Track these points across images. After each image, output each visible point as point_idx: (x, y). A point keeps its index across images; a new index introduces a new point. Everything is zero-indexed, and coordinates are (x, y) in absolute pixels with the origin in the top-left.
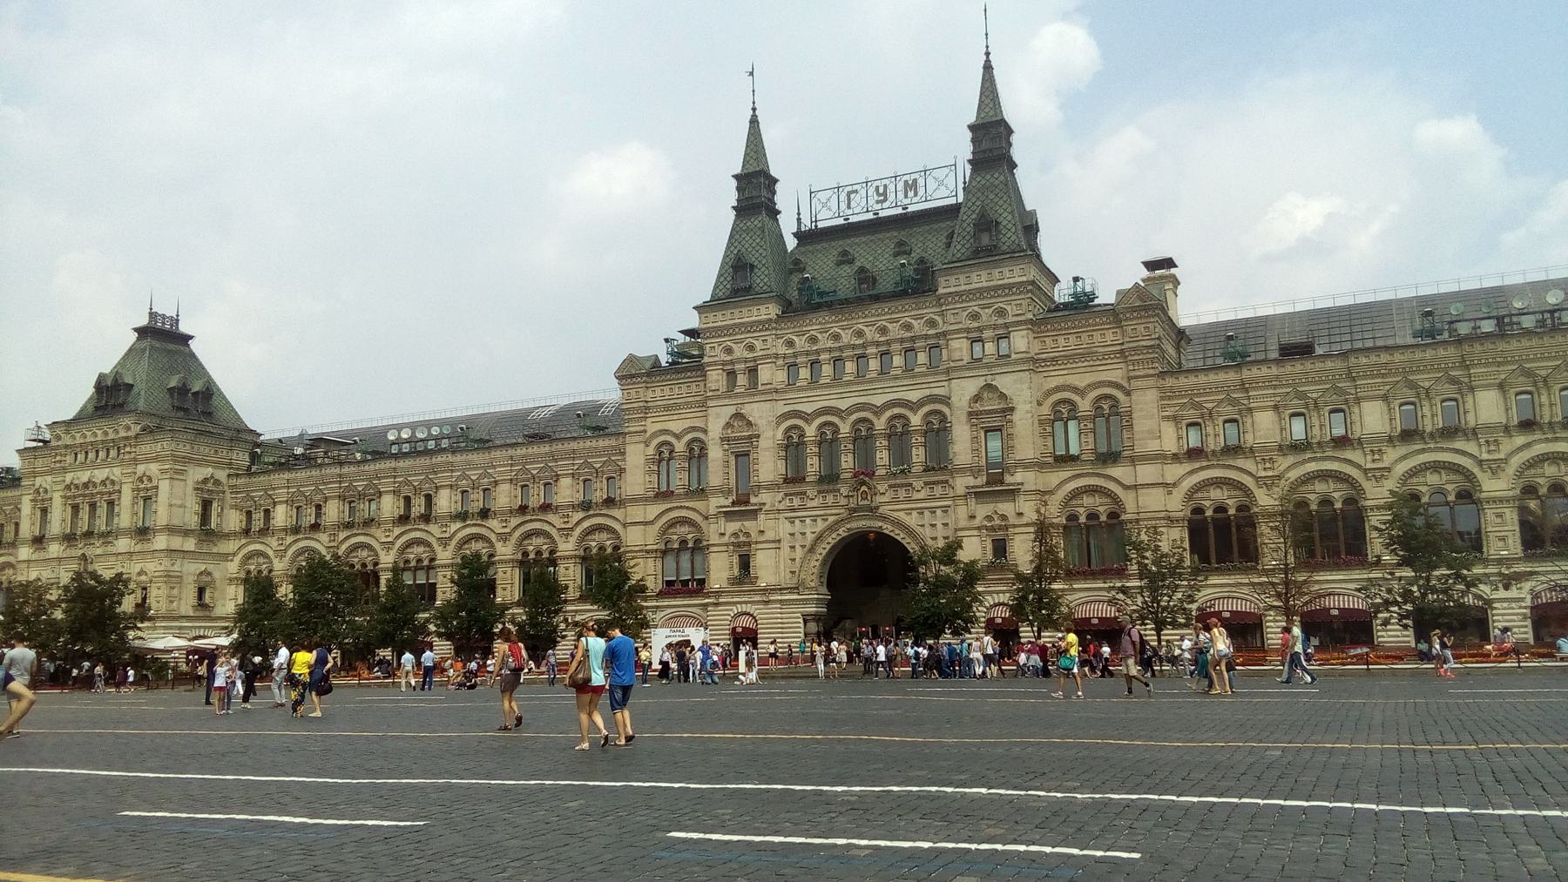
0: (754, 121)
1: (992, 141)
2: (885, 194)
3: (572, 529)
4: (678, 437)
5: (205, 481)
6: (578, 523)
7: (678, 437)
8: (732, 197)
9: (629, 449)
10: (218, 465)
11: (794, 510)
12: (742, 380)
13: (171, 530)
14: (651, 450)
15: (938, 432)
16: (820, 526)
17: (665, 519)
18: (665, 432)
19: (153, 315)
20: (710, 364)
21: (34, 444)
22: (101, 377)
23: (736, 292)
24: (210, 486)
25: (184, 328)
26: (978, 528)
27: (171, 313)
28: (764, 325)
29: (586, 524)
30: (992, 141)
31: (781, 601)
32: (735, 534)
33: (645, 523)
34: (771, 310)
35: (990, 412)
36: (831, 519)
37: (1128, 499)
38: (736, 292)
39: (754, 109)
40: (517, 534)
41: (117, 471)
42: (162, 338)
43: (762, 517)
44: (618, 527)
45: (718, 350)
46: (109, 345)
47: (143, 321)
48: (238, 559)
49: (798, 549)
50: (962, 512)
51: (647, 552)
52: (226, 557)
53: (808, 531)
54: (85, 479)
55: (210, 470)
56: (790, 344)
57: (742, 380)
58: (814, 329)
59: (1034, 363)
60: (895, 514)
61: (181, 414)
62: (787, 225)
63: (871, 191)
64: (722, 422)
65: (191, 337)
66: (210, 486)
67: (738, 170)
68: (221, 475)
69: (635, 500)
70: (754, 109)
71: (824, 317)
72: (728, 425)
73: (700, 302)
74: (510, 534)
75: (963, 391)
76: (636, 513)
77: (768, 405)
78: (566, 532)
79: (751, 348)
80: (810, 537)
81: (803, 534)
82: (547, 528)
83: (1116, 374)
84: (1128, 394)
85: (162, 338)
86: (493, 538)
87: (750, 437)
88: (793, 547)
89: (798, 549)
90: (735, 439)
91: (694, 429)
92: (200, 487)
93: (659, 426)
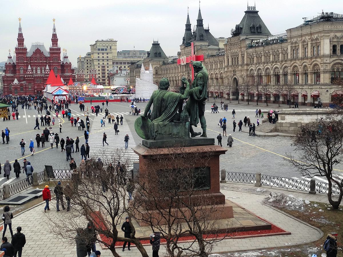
0: (188, 16)
1: (200, 22)
5: (156, 67)
8: (185, 28)
10: (158, 65)
24: (157, 68)
25: (159, 43)
30: (200, 22)
55: (157, 65)
61: (156, 57)
62: (192, 31)
66: (157, 68)
67: (186, 24)
68: (158, 66)
73: (180, 45)
92: (155, 68)
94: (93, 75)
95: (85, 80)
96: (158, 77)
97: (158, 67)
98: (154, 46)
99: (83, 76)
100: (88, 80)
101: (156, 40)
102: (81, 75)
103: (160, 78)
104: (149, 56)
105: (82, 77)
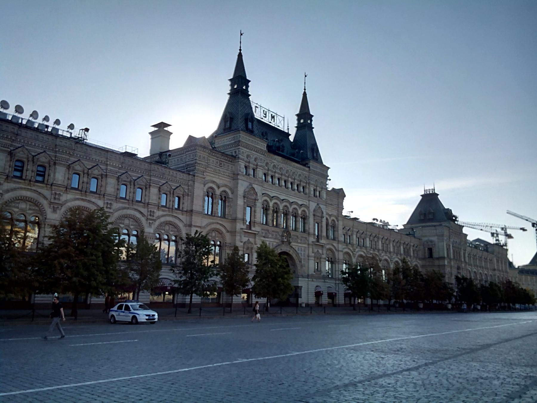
2: (266, 114)
3: (155, 220)
6: (159, 217)
7: (219, 187)
9: (197, 185)
11: (264, 237)
15: (305, 218)
18: (214, 182)
26: (315, 257)
29: (163, 220)
34: (263, 146)
35: (318, 216)
36: (275, 243)
37: (336, 253)
39: (240, 50)
43: (257, 238)
44: (181, 225)
45: (245, 155)
50: (311, 250)
59: (326, 204)
60: (294, 247)
63: (262, 111)
70: (240, 50)
75: (313, 205)
77: (260, 188)
82: (138, 215)
83: (335, 213)
84: (338, 221)
91: (226, 186)
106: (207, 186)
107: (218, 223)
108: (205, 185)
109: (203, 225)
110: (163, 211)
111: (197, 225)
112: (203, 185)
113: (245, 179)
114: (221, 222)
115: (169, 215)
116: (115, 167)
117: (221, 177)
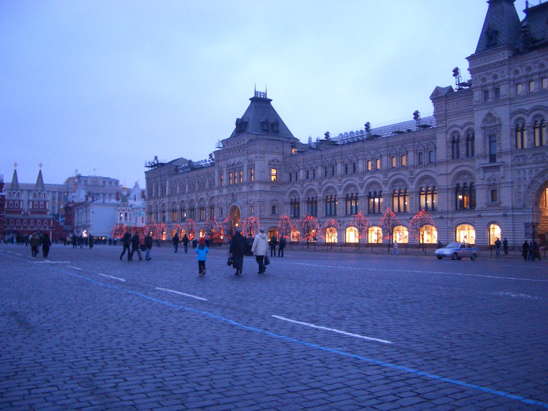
4: (462, 128)
5: (273, 161)
7: (462, 128)
11: (519, 165)
12: (491, 94)
13: (260, 182)
14: (449, 136)
16: (534, 174)
17: (456, 172)
19: (256, 93)
20: (474, 88)
21: (217, 149)
22: (238, 120)
23: (488, 46)
25: (269, 97)
27: (263, 91)
28: (501, 63)
31: (513, 215)
32: (489, 180)
33: (447, 174)
34: (505, 55)
36: (540, 169)
38: (488, 46)
40: (391, 181)
41: (242, 158)
42: (260, 103)
43: (502, 169)
46: (241, 107)
47: (253, 95)
48: (288, 194)
49: (522, 187)
51: (447, 189)
52: (283, 193)
53: (527, 177)
54: (232, 162)
55: (275, 156)
56: (517, 72)
57: (491, 94)
58: (529, 63)
64: (481, 119)
65: (271, 100)
69: (441, 163)
71: (535, 53)
72: (485, 120)
73: (469, 55)
74: (388, 181)
76: (442, 169)
78: (412, 180)
79: (495, 77)
80: (528, 180)
81: (525, 178)
85: (260, 103)
86: (381, 183)
87: (496, 126)
88: (520, 186)
89: (522, 187)
90: (487, 127)
93: (452, 123)
94: (39, 202)
95: (23, 213)
96: (279, 190)
97: (278, 161)
98: (257, 104)
99: (20, 204)
100: (29, 213)
101: (261, 89)
102: (14, 201)
103: (283, 193)
104: (244, 130)
105: (17, 205)
106: (450, 132)
107: (464, 165)
108: (447, 133)
109: (449, 171)
110: (420, 168)
111: (443, 173)
112: (444, 134)
113: (483, 107)
114: (467, 163)
115: (424, 171)
116: (384, 148)
117: (464, 117)
